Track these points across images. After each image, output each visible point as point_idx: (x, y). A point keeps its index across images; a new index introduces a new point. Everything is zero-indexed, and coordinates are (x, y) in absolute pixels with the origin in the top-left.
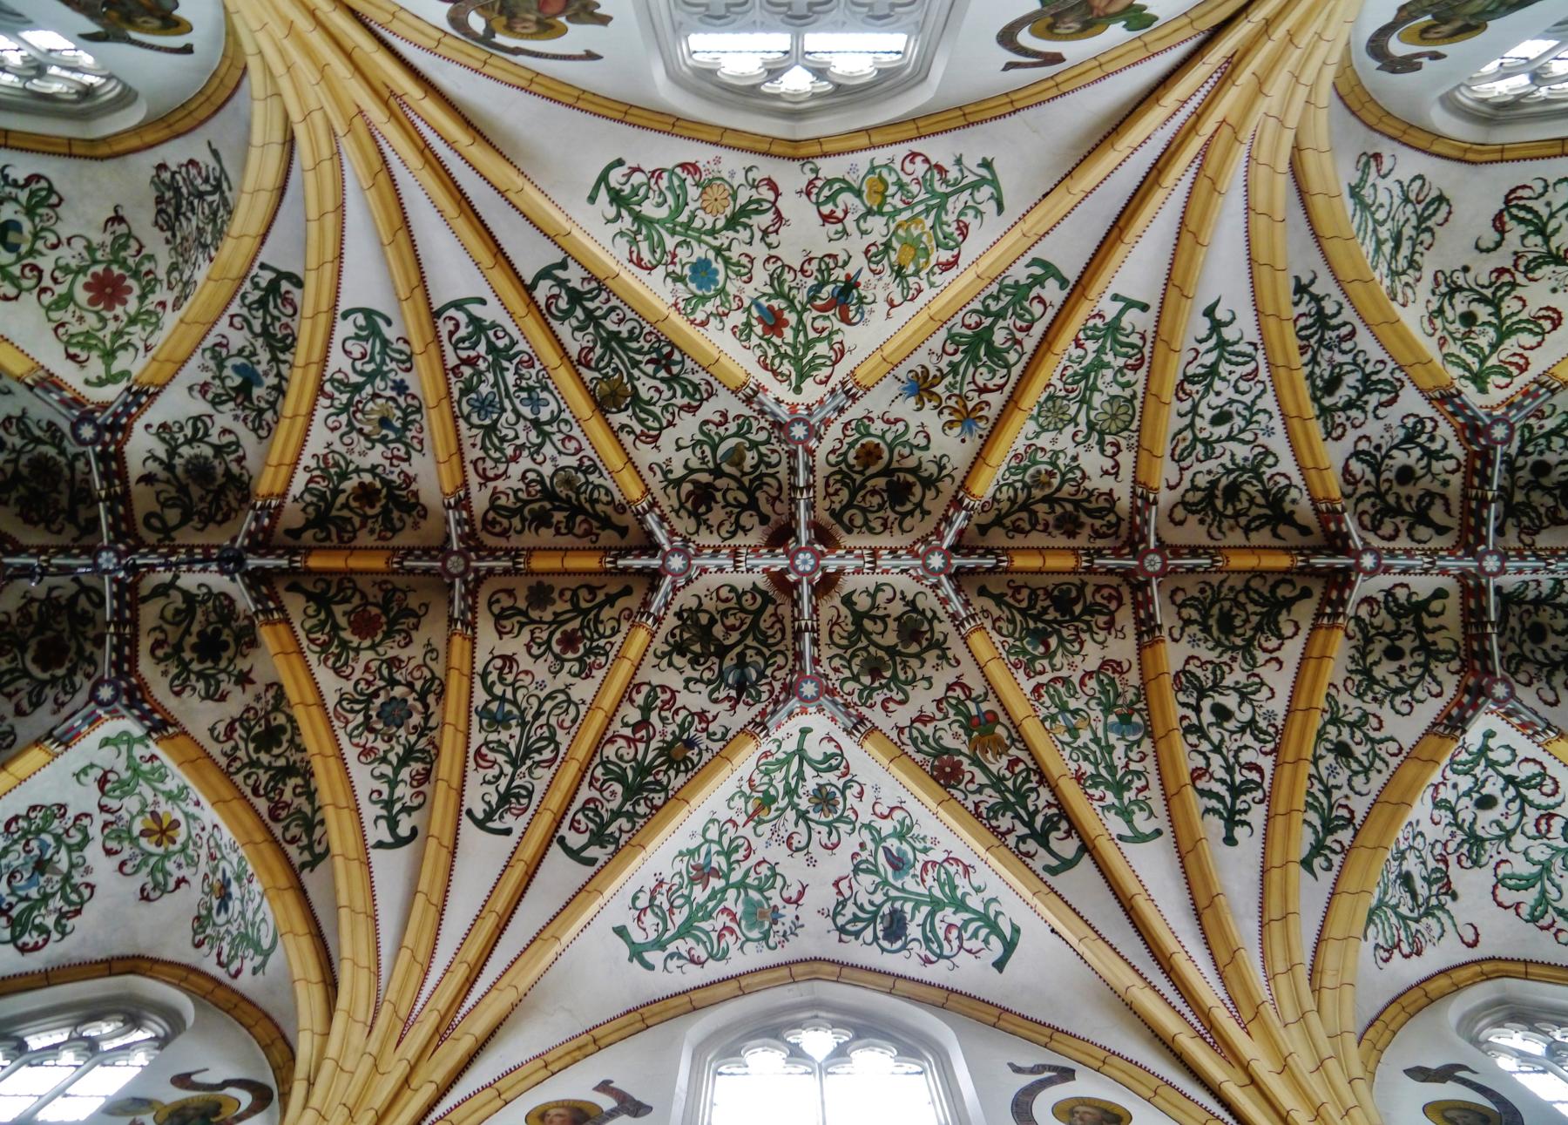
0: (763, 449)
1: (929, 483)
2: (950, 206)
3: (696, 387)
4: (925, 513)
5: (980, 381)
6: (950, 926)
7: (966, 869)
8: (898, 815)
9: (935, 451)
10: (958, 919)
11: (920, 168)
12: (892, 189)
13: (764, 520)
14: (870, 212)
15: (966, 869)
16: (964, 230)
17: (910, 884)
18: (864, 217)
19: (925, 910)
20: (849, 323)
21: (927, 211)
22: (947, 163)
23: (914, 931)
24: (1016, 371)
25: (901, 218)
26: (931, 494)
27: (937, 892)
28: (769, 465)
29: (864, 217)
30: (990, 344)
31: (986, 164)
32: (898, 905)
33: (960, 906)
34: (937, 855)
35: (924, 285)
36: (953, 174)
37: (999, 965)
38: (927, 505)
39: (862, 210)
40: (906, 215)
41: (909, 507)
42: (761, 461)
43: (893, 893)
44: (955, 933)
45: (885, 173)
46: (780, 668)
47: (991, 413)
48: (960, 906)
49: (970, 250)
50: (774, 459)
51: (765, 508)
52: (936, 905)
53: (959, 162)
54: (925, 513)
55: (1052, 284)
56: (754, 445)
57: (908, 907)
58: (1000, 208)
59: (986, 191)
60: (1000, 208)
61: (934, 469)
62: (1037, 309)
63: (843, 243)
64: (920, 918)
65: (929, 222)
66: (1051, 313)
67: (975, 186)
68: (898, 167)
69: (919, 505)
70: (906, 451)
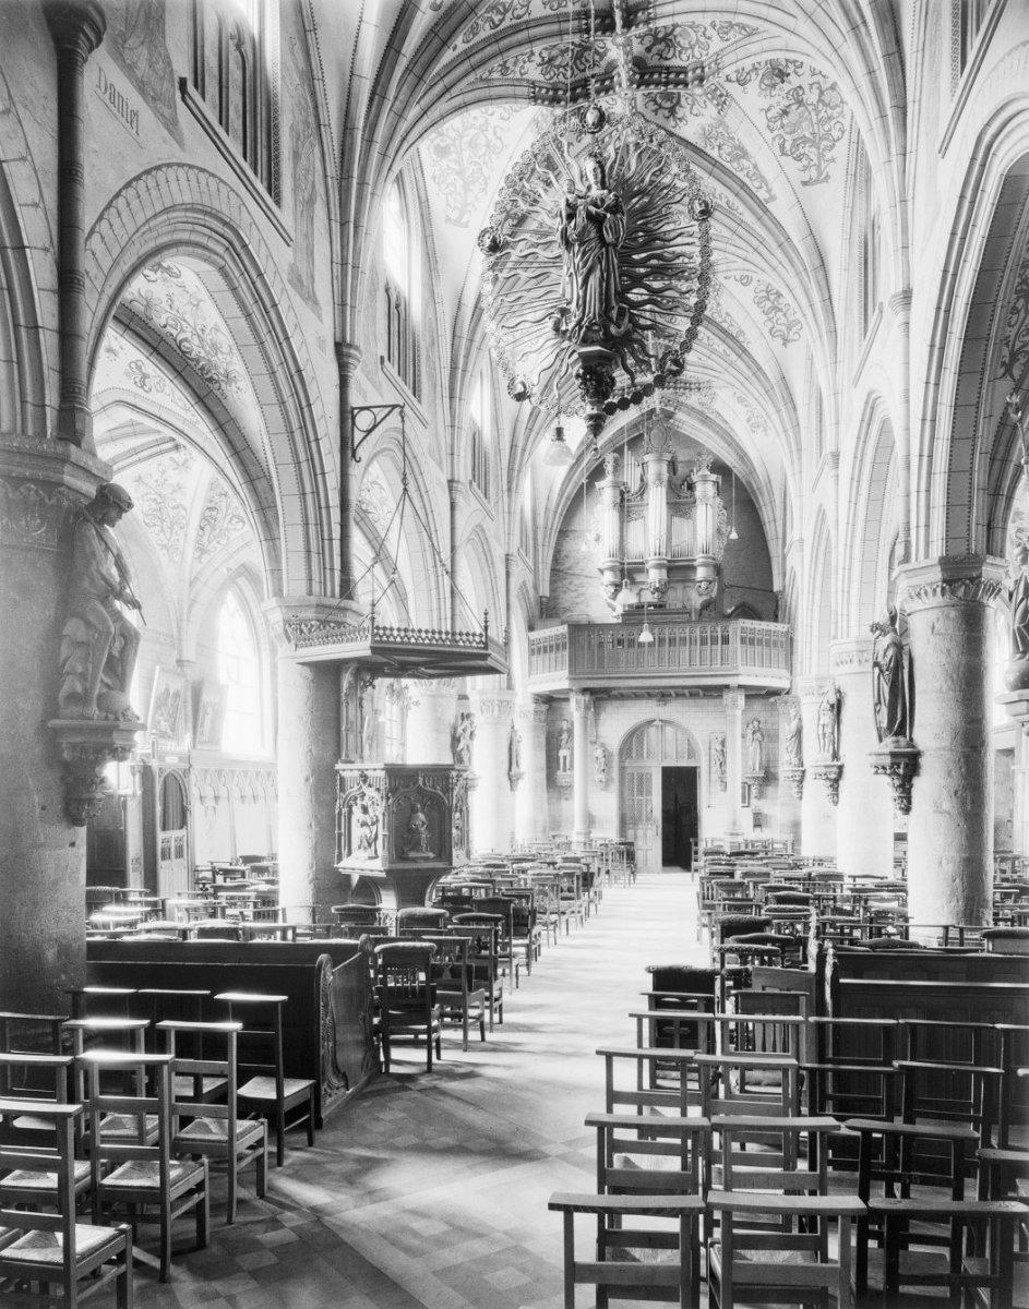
0: (689, 51)
1: (672, 111)
2: (813, 149)
3: (727, 33)
4: (656, 111)
5: (725, 147)
6: (453, 184)
7: (484, 189)
8: (498, 143)
9: (690, 117)
10: (460, 189)
11: (836, 134)
12: (829, 111)
13: (648, 50)
14: (822, 93)
15: (484, 189)
16: (798, 159)
17: (466, 154)
18: (820, 88)
19: (457, 167)
20: (762, 81)
21: (813, 134)
22: (834, 153)
23: (444, 163)
24: (728, 165)
25: (813, 113)
26: (667, 113)
27: (468, 173)
28: (680, 52)
29: (820, 88)
30: (743, 157)
31: (828, 177)
32: (452, 149)
33: (467, 190)
34: (485, 171)
35: (776, 133)
36: (828, 155)
37: (448, 219)
38: (660, 111)
39: (824, 87)
40: (815, 120)
41: (659, 101)
42: (683, 48)
43: (457, 142)
44: (452, 188)
45: (838, 109)
46: (564, 75)
47: (708, 150)
48: (467, 190)
49: (788, 161)
50: (684, 57)
51: (655, 50)
52: (460, 173)
53: (833, 160)
54: (656, 111)
55: (766, 196)
56: (692, 48)
57: (454, 156)
58: (805, 183)
59: (813, 173)
60: (805, 183)
61: (678, 116)
62: (757, 184)
63: (808, 73)
64: (452, 165)
65: (808, 135)
66: (754, 190)
67: (819, 166)
68: (840, 119)
69: (660, 107)
70: (690, 101)
